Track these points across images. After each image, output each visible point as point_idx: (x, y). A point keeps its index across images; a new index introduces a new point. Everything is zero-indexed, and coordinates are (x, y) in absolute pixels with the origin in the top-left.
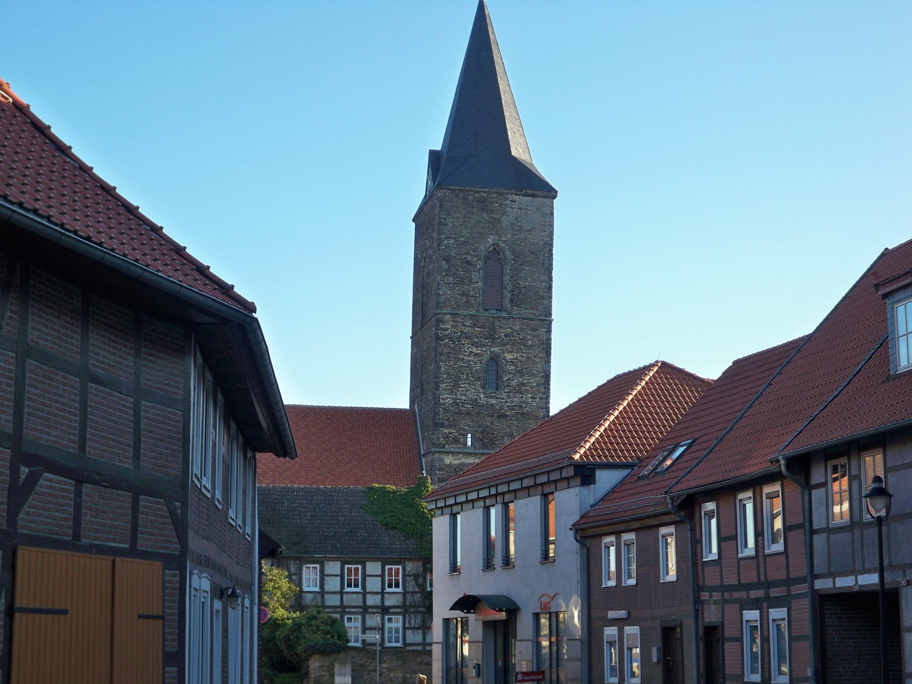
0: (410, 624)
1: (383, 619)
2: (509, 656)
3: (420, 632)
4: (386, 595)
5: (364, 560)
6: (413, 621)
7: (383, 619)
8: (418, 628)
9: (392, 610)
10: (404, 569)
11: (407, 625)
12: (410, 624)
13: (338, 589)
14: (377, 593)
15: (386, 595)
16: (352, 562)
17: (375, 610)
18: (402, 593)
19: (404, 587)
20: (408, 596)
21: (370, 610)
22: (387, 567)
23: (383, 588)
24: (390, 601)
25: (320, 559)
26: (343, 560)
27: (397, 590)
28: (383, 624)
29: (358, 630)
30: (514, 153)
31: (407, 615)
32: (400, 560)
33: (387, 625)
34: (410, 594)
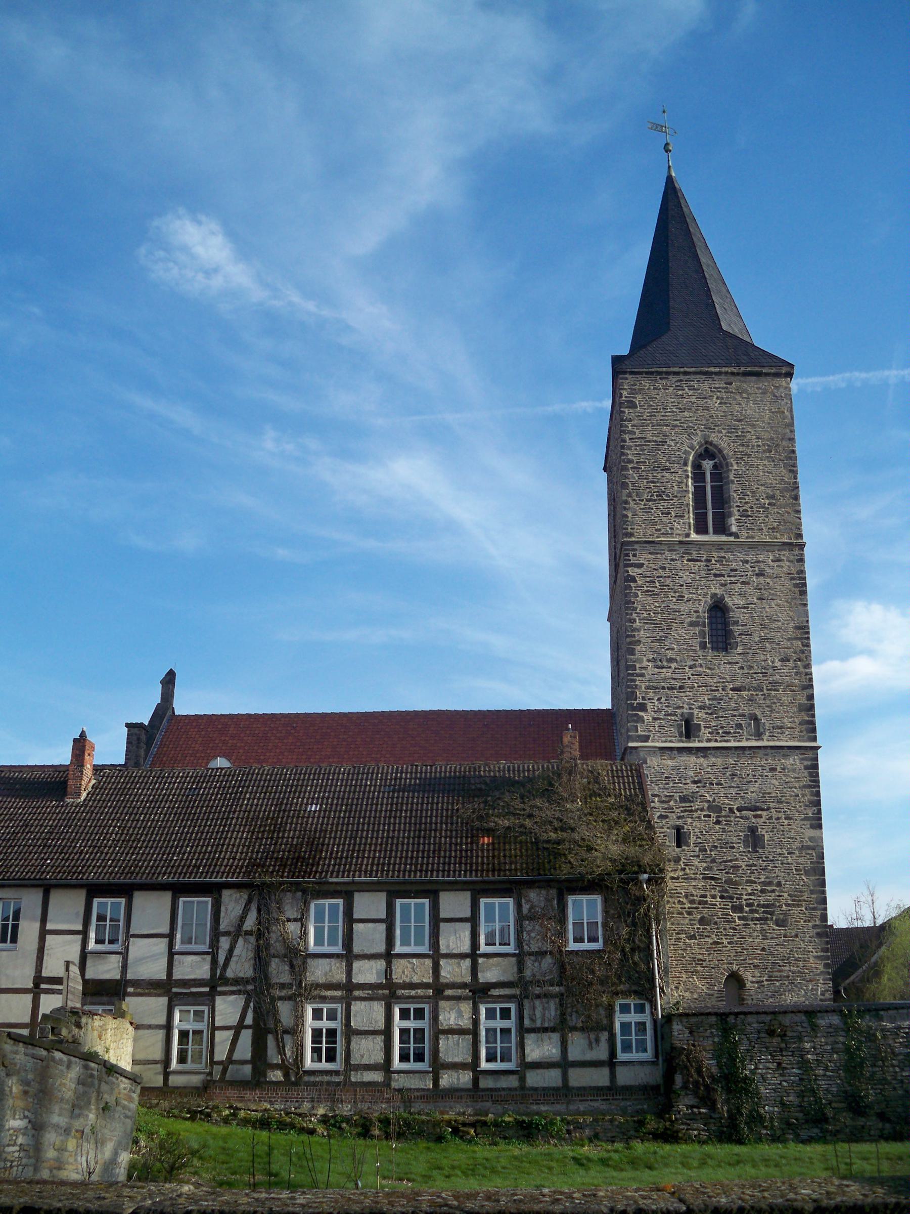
0: (533, 1020)
1: (476, 1011)
2: (539, 887)
3: (556, 1037)
4: (481, 960)
5: (434, 887)
6: (538, 1014)
7: (476, 1011)
8: (553, 1030)
9: (495, 992)
10: (519, 906)
11: (527, 1023)
12: (533, 1020)
13: (381, 948)
14: (462, 956)
15: (481, 960)
16: (411, 891)
17: (459, 992)
18: (513, 955)
19: (519, 943)
20: (529, 962)
21: (449, 992)
22: (483, 901)
23: (613, 1054)
24: (490, 973)
25: (344, 888)
26: (392, 888)
27: (642, 1056)
28: (476, 1022)
29: (207, 906)
30: (725, 327)
31: (526, 1003)
32: (508, 886)
33: (483, 1024)
34: (532, 958)
